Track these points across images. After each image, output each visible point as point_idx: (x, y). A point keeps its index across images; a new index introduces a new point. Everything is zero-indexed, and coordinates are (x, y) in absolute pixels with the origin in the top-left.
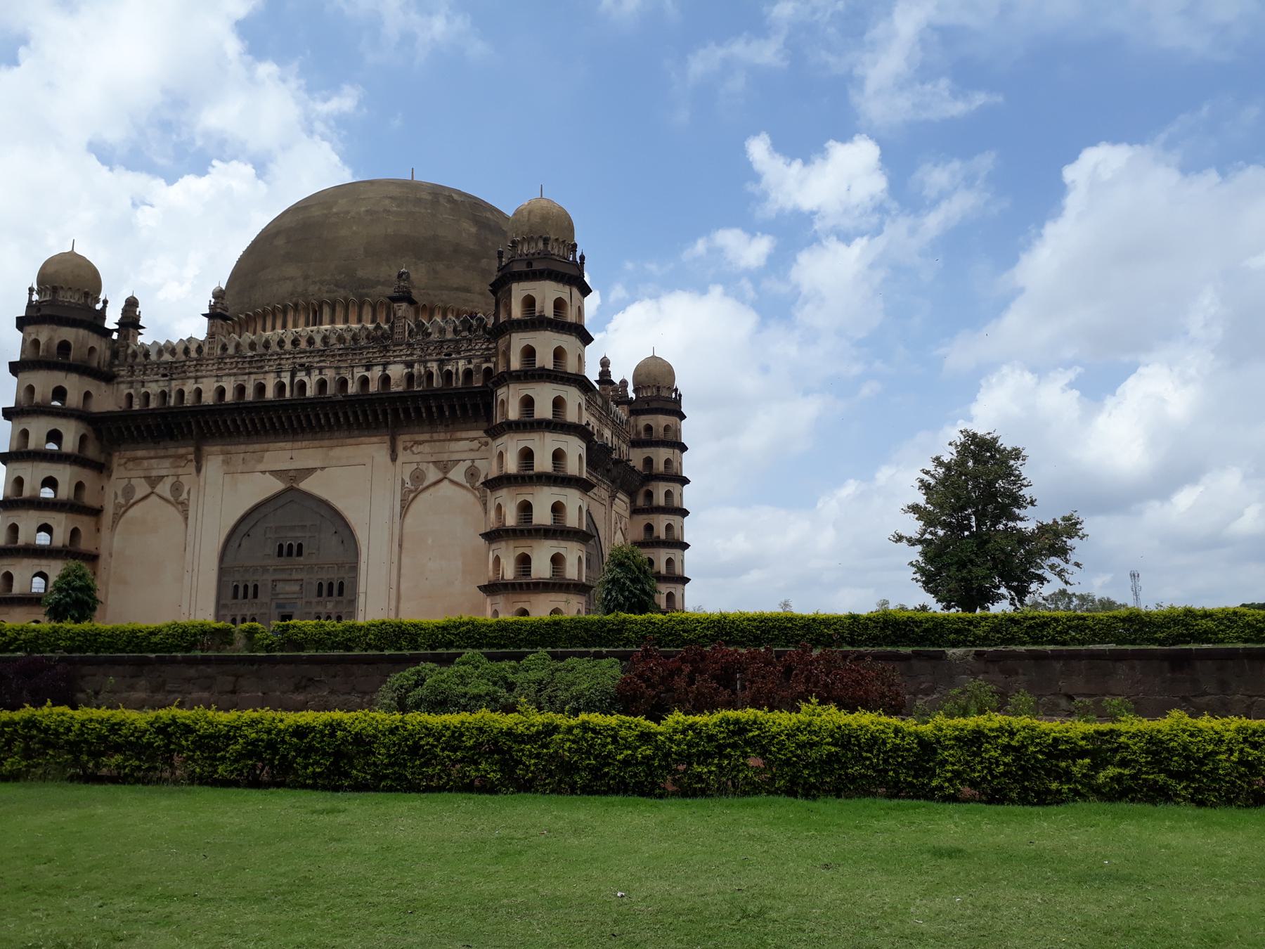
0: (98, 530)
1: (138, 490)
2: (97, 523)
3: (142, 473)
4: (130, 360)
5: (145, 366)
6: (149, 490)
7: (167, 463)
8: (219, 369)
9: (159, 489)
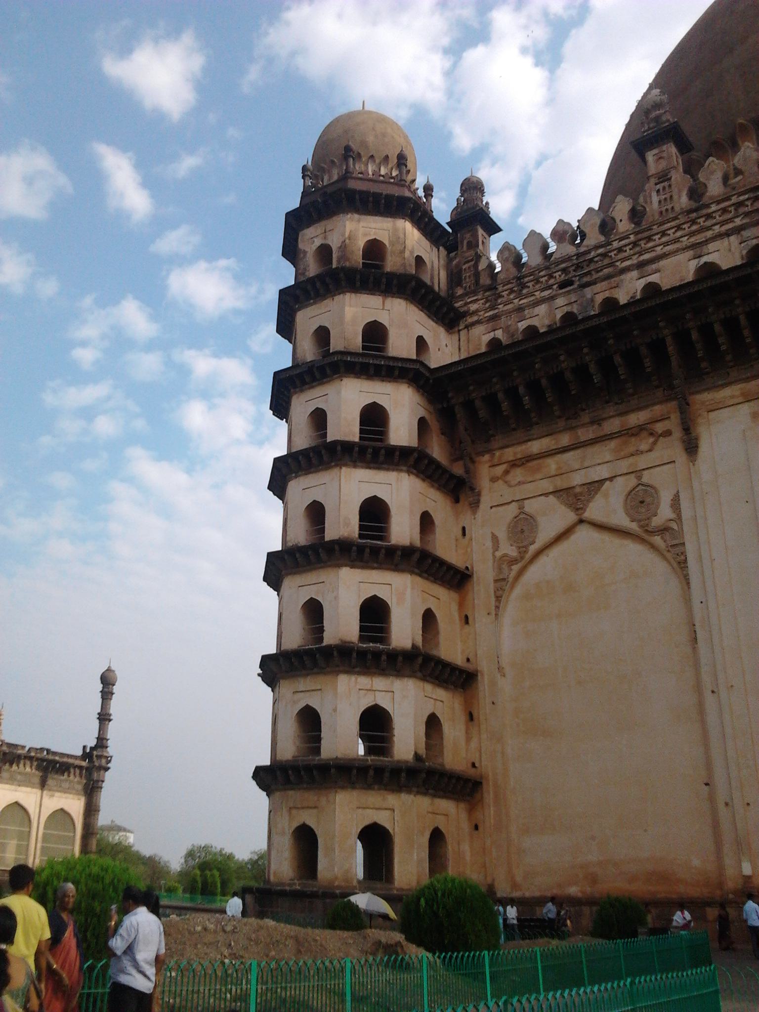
0: (466, 620)
1: (542, 521)
2: (461, 605)
3: (547, 485)
4: (485, 280)
5: (519, 278)
6: (572, 517)
7: (605, 452)
8: (692, 234)
9: (595, 510)
